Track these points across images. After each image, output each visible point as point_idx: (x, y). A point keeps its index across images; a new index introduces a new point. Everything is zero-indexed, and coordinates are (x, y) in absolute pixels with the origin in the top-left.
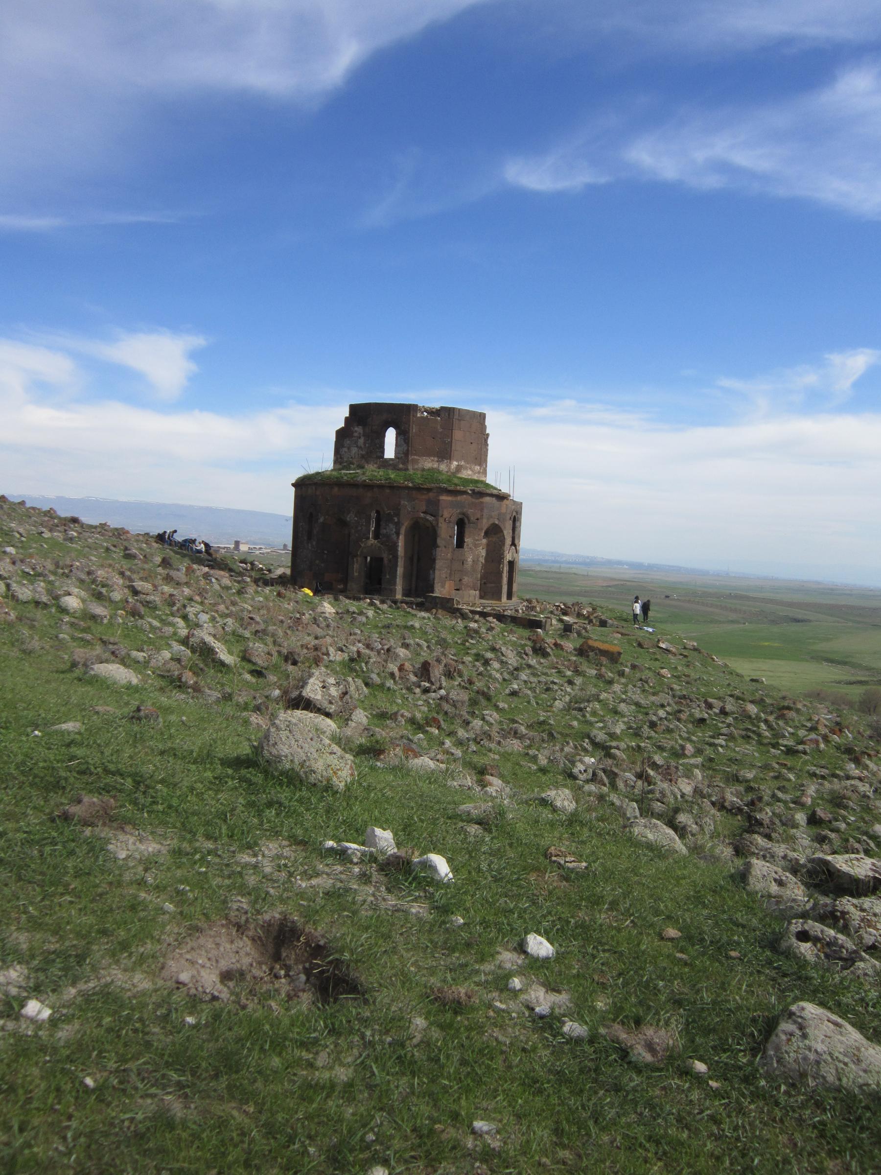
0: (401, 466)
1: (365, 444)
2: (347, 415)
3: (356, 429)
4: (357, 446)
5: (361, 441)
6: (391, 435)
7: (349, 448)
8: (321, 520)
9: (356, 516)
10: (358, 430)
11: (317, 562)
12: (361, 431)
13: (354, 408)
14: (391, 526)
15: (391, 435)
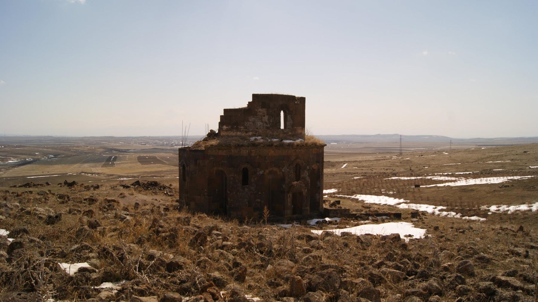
0: (290, 133)
1: (269, 119)
2: (251, 100)
3: (260, 110)
4: (262, 121)
5: (266, 118)
6: (282, 113)
7: (253, 122)
8: (261, 172)
9: (288, 168)
10: (261, 111)
11: (259, 200)
12: (265, 112)
13: (254, 96)
14: (306, 171)
15: (282, 113)
